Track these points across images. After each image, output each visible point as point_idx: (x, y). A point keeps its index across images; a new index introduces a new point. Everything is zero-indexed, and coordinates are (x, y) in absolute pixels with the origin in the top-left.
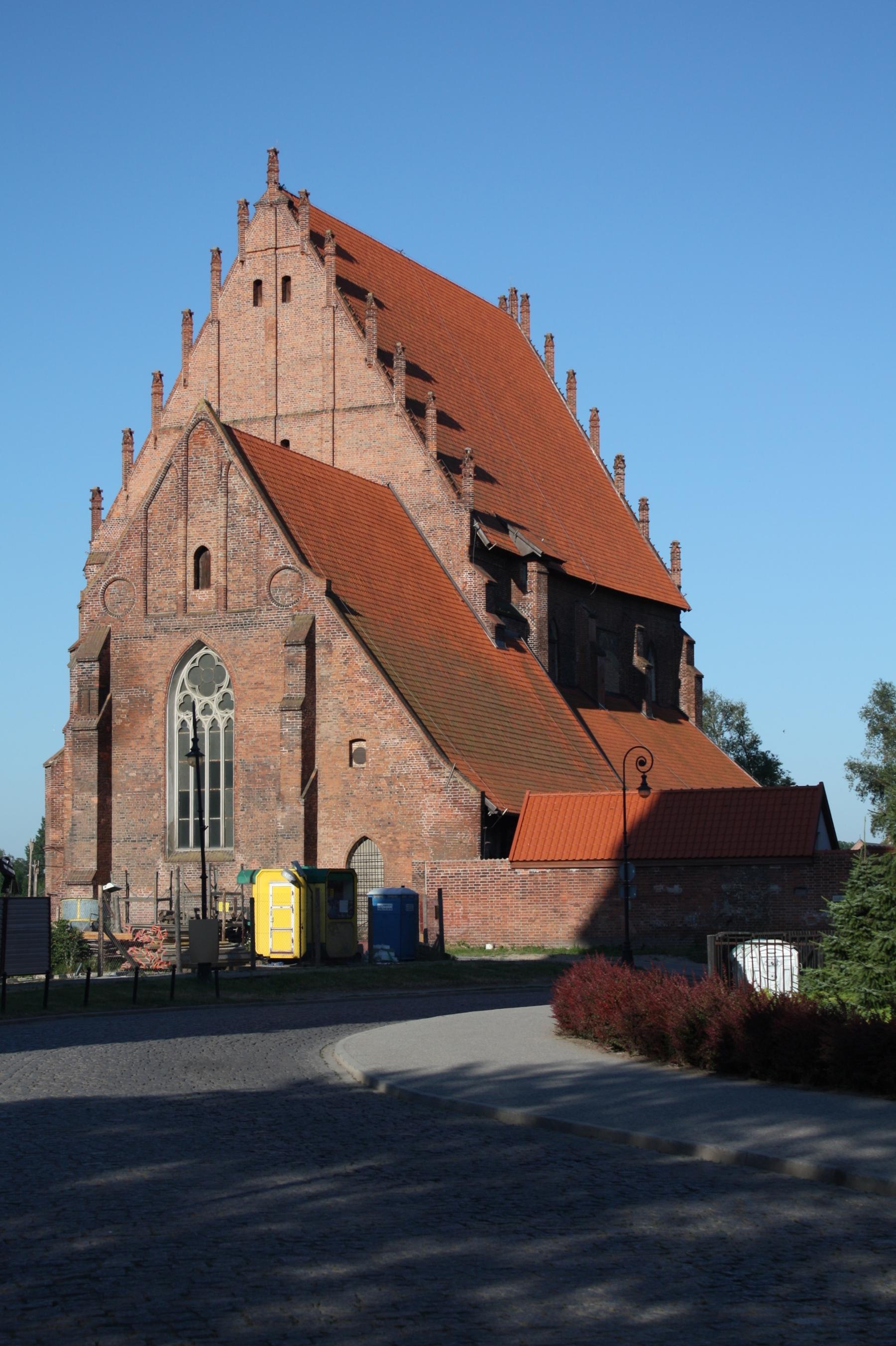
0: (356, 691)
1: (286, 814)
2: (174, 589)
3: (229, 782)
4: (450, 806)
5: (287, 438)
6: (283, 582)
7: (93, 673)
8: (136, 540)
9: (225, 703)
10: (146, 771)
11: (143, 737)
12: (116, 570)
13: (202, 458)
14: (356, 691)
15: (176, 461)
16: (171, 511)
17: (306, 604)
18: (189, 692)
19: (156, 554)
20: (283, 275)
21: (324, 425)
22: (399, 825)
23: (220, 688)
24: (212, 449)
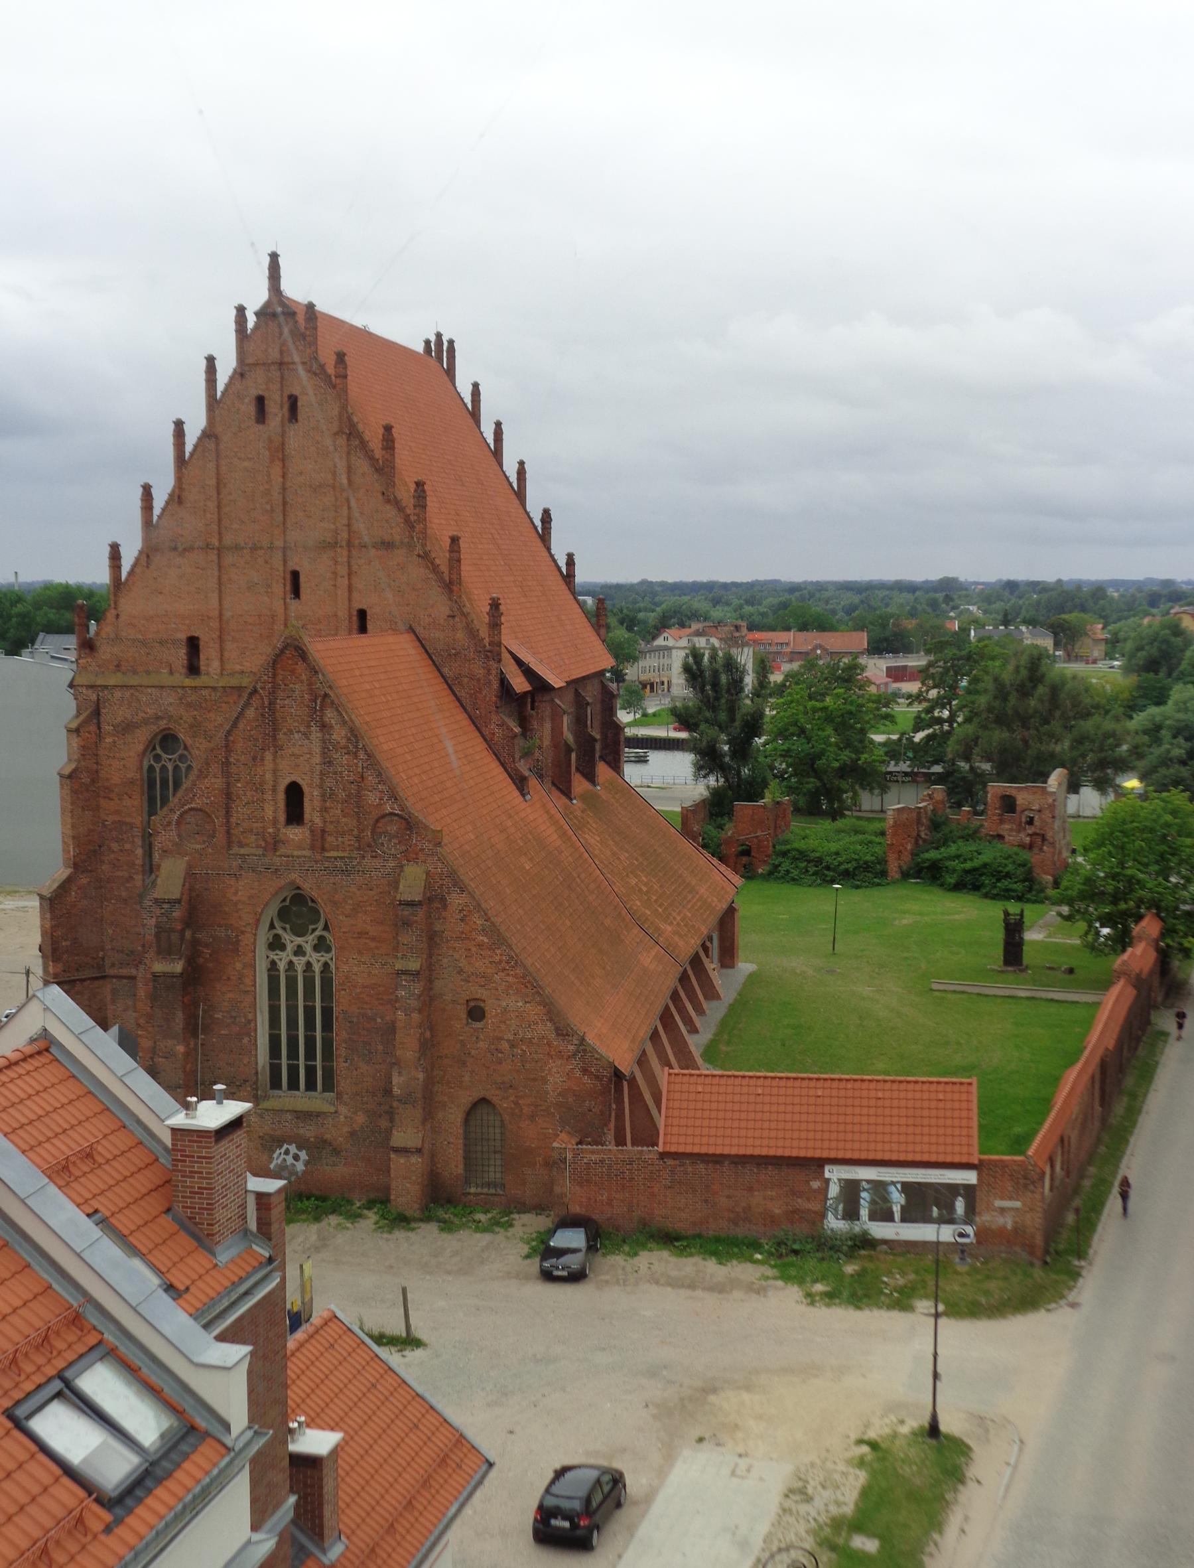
0: (474, 949)
1: (402, 1079)
2: (261, 825)
3: (327, 1026)
4: (578, 1074)
5: (298, 569)
6: (389, 828)
7: (174, 914)
8: (215, 768)
9: (321, 945)
10: (234, 1014)
11: (229, 979)
12: (193, 799)
13: (291, 686)
14: (474, 949)
16: (257, 740)
17: (417, 854)
18: (280, 932)
19: (239, 785)
20: (289, 393)
21: (339, 559)
22: (521, 1089)
23: (314, 930)
24: (304, 677)
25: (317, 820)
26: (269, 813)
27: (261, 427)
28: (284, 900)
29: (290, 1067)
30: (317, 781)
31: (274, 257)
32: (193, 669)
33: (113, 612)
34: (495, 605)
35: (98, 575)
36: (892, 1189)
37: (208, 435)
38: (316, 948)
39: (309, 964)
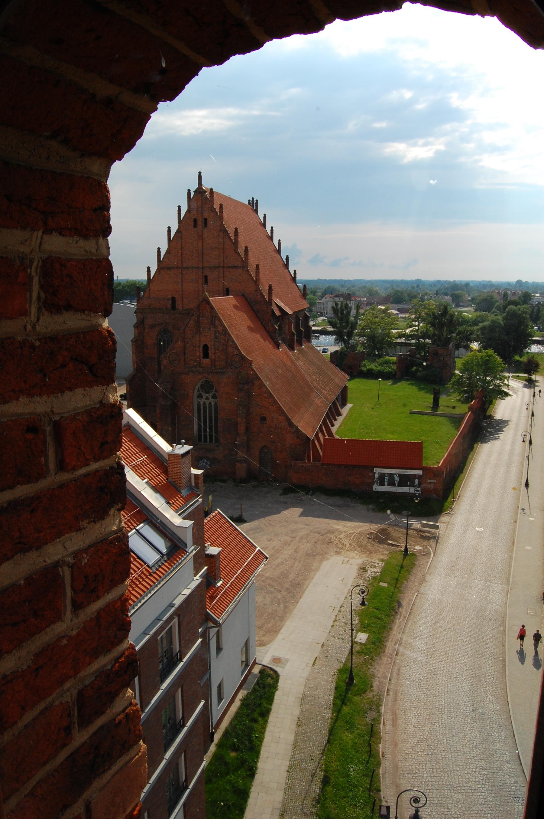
9: (214, 397)
15: (195, 314)
18: (201, 392)
23: (212, 392)
24: (209, 311)
25: (213, 357)
26: (198, 354)
27: (195, 229)
28: (202, 382)
29: (204, 435)
30: (213, 344)
31: (200, 173)
32: (174, 307)
33: (148, 289)
34: (270, 287)
35: (144, 277)
36: (395, 476)
37: (178, 231)
38: (213, 398)
39: (210, 403)
